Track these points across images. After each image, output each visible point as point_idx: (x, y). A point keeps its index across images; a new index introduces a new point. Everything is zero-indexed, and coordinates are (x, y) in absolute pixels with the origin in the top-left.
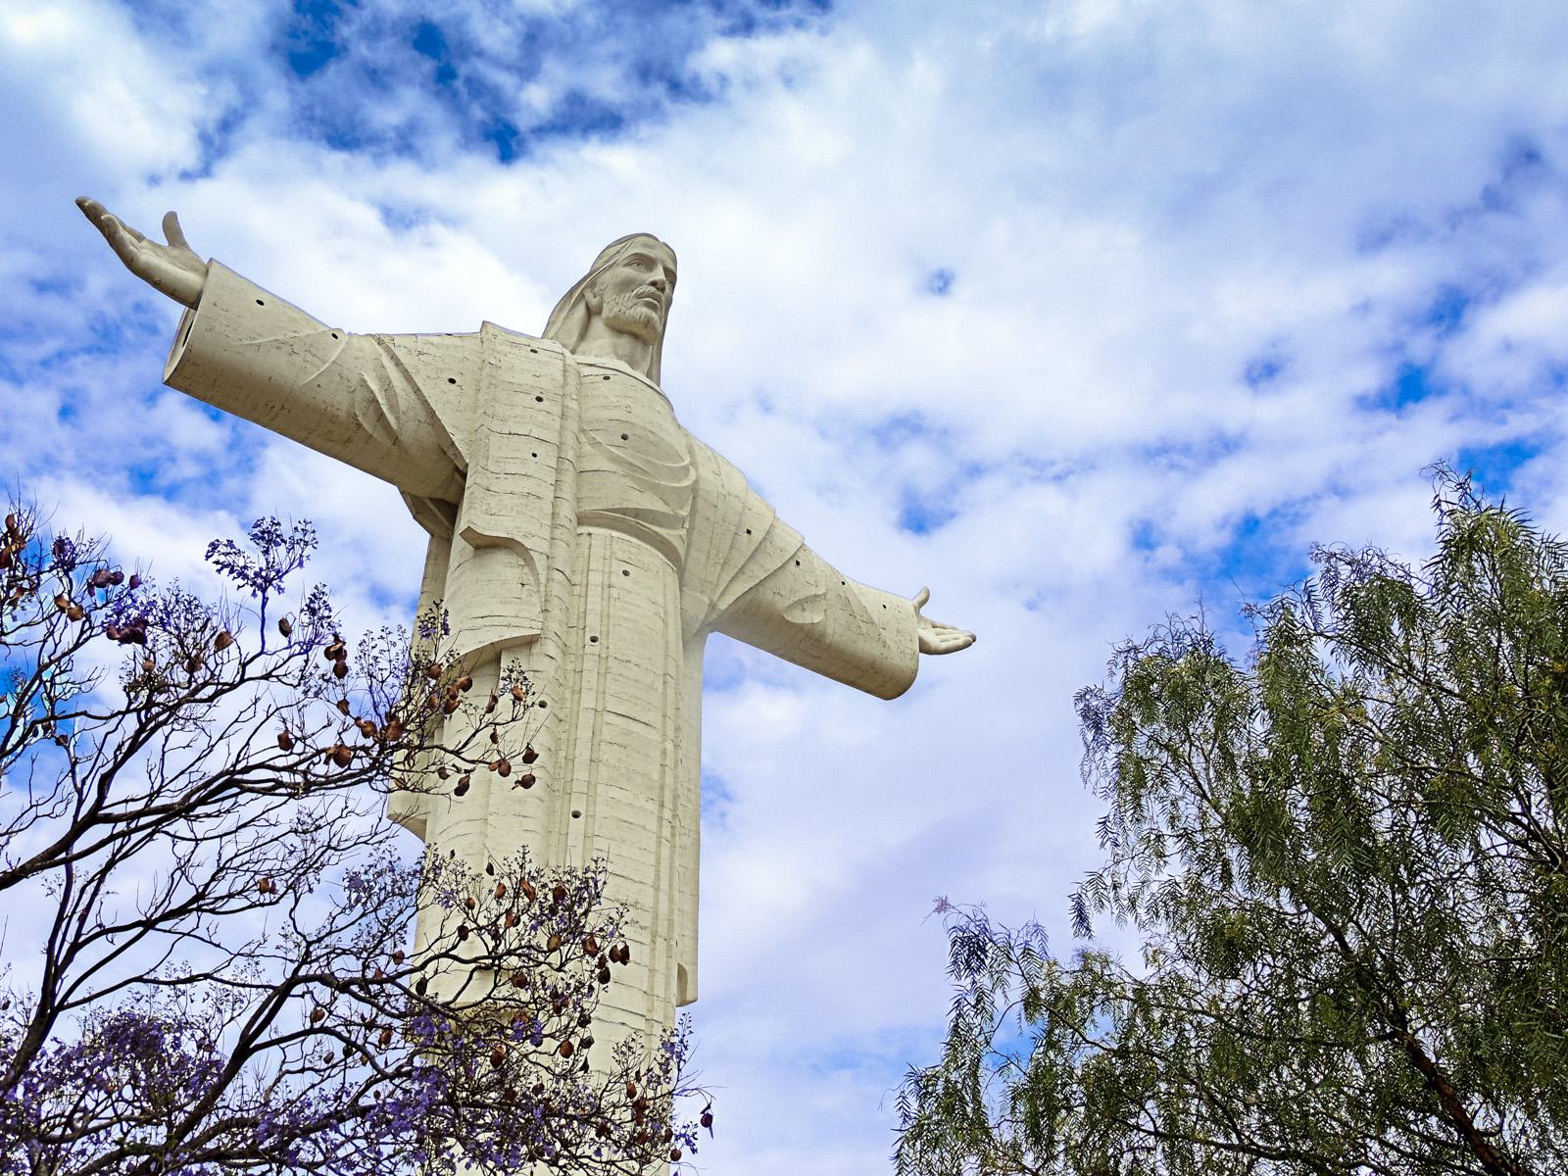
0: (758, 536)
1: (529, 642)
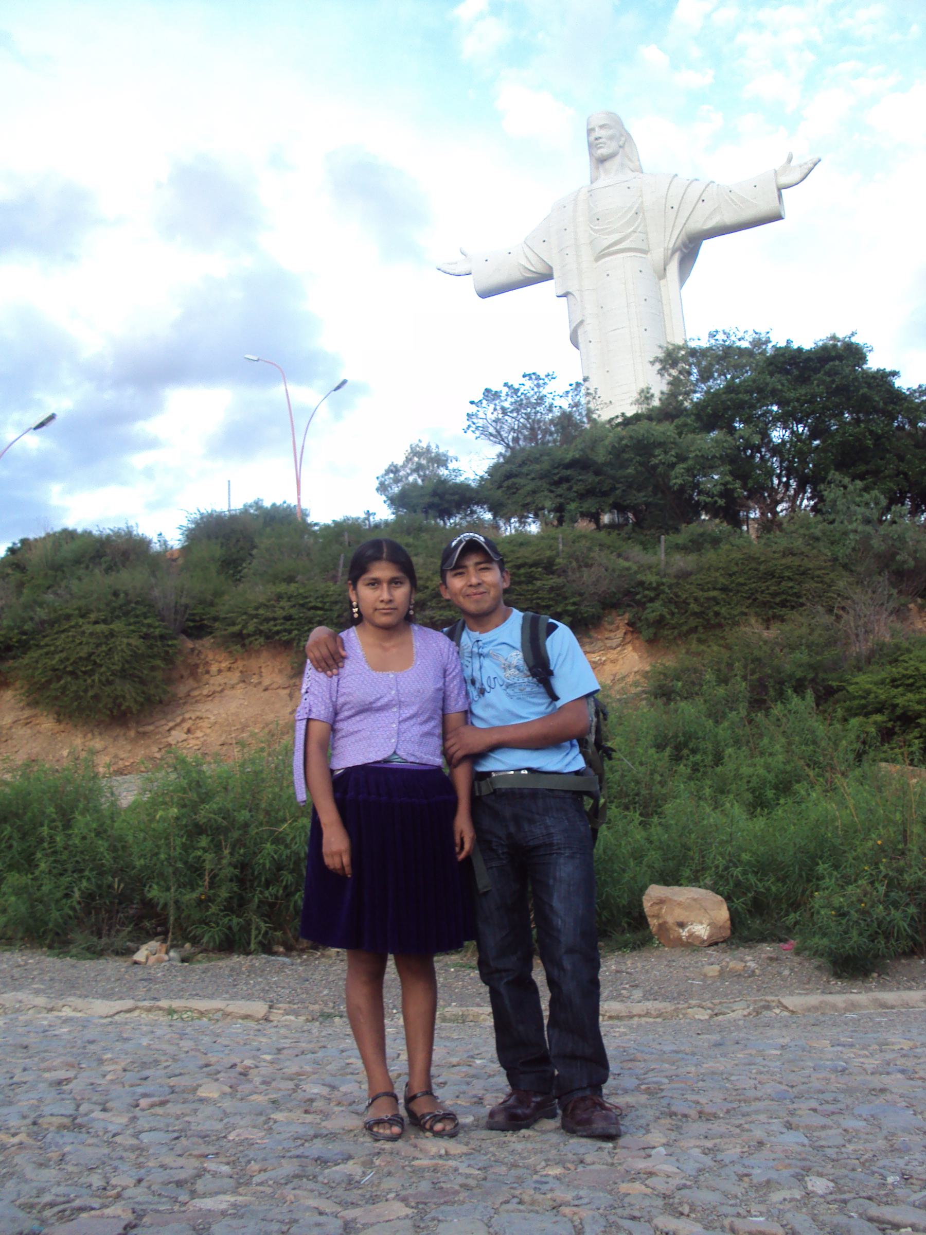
0: (676, 207)
1: (582, 322)
